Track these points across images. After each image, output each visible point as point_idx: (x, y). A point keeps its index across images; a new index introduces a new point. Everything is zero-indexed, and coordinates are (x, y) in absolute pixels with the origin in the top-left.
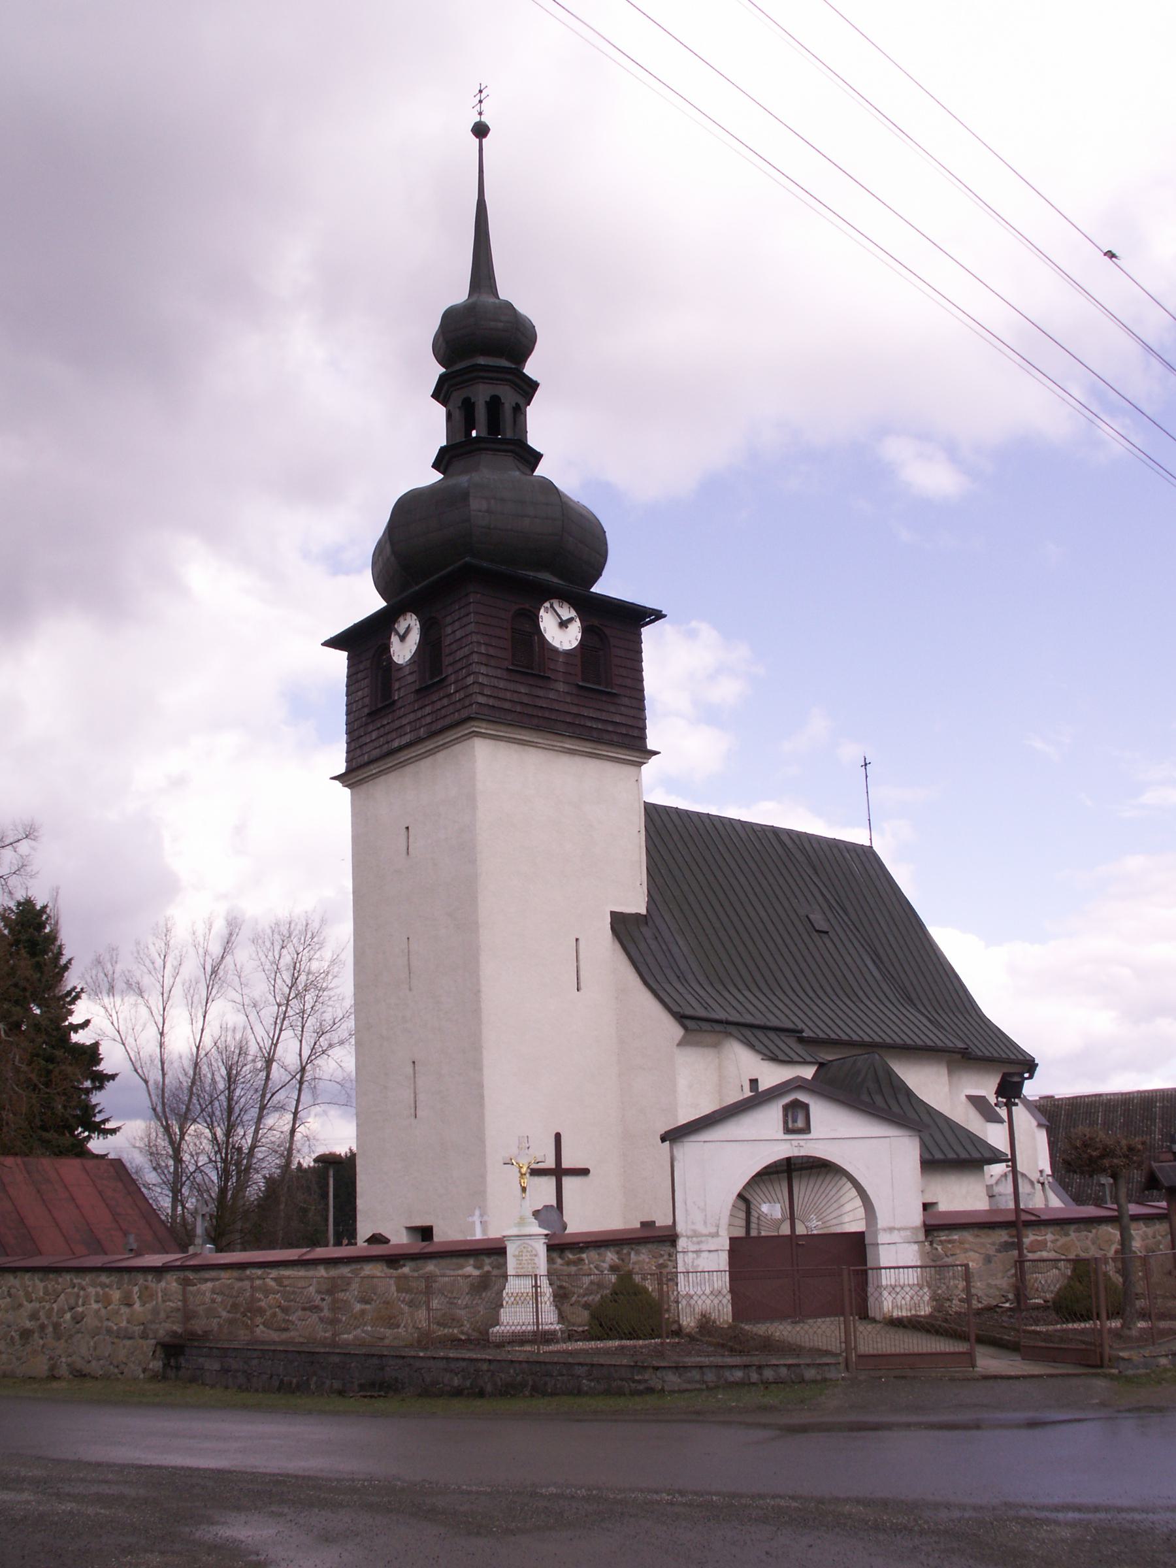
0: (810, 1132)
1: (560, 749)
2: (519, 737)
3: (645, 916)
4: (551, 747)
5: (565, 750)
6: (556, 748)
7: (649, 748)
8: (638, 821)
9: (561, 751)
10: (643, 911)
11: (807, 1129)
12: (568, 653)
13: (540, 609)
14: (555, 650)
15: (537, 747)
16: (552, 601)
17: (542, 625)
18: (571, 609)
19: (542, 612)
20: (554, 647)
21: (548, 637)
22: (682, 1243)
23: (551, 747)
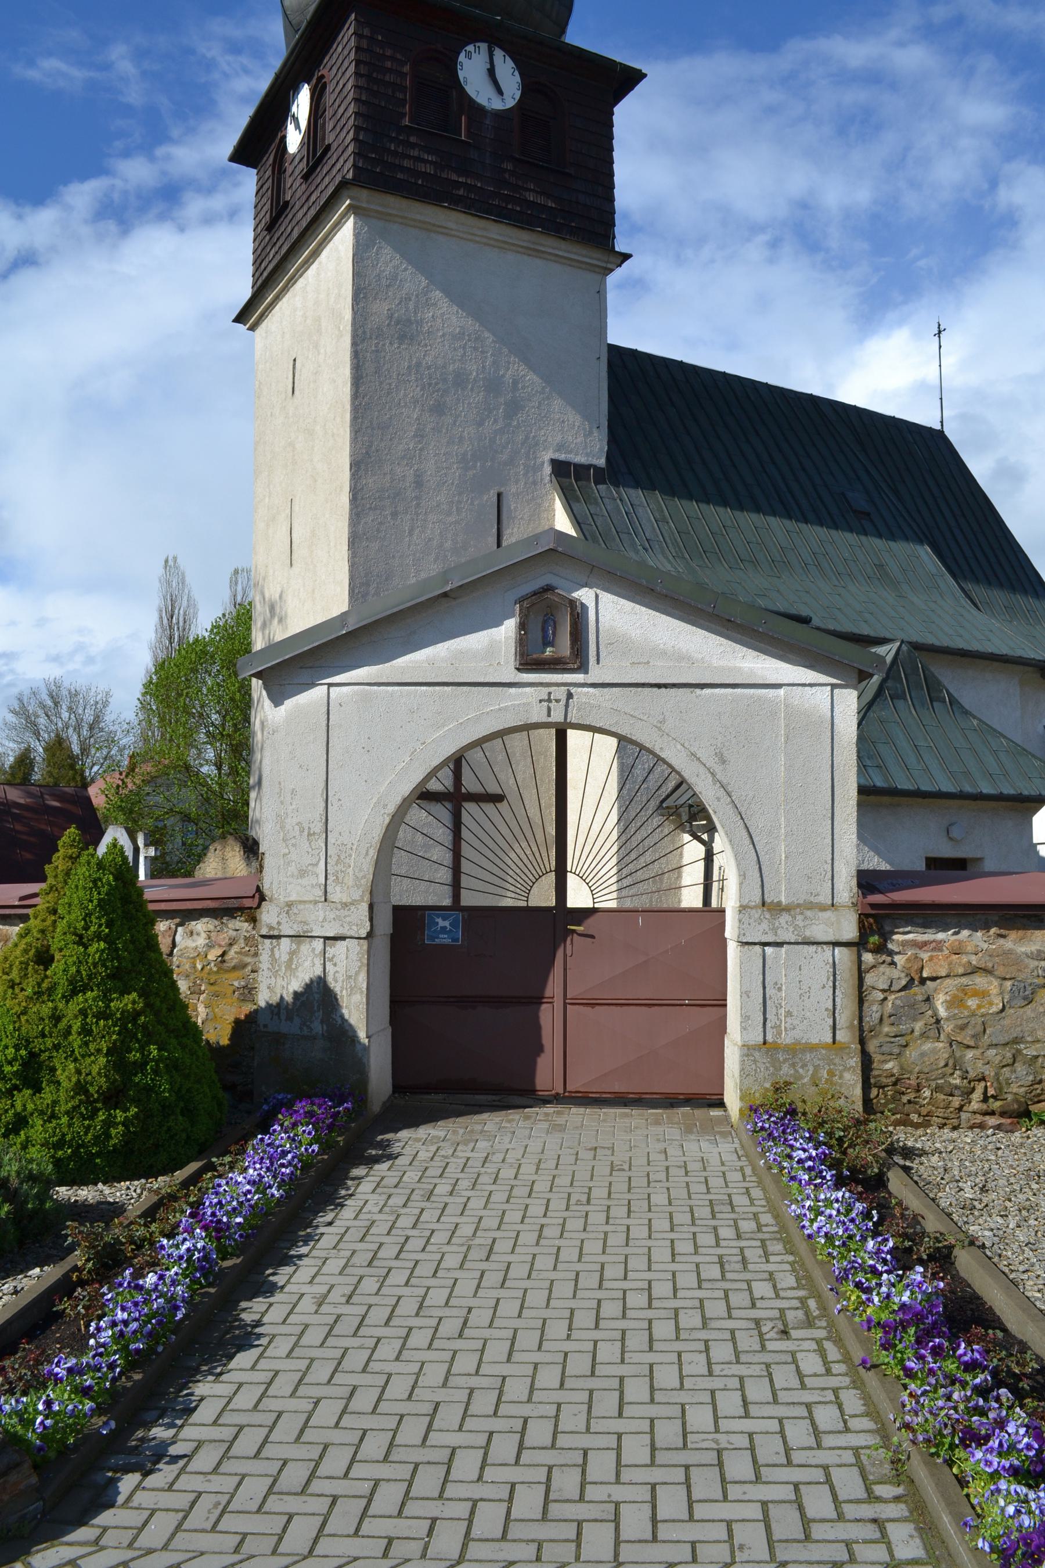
0: (583, 668)
1: (485, 240)
2: (418, 217)
3: (603, 469)
4: (470, 237)
5: (492, 242)
6: (478, 239)
7: (617, 249)
8: (605, 350)
9: (486, 244)
10: (601, 462)
11: (578, 660)
12: (498, 115)
13: (459, 54)
14: (481, 109)
15: (447, 234)
16: (477, 44)
17: (461, 75)
18: (507, 58)
19: (462, 57)
20: (479, 104)
21: (471, 90)
22: (268, 915)
23: (470, 237)
